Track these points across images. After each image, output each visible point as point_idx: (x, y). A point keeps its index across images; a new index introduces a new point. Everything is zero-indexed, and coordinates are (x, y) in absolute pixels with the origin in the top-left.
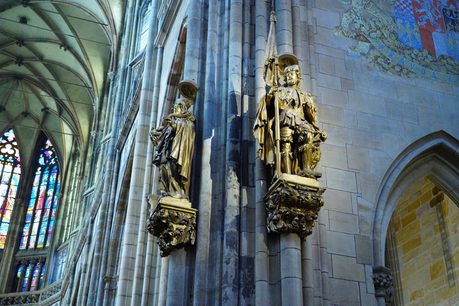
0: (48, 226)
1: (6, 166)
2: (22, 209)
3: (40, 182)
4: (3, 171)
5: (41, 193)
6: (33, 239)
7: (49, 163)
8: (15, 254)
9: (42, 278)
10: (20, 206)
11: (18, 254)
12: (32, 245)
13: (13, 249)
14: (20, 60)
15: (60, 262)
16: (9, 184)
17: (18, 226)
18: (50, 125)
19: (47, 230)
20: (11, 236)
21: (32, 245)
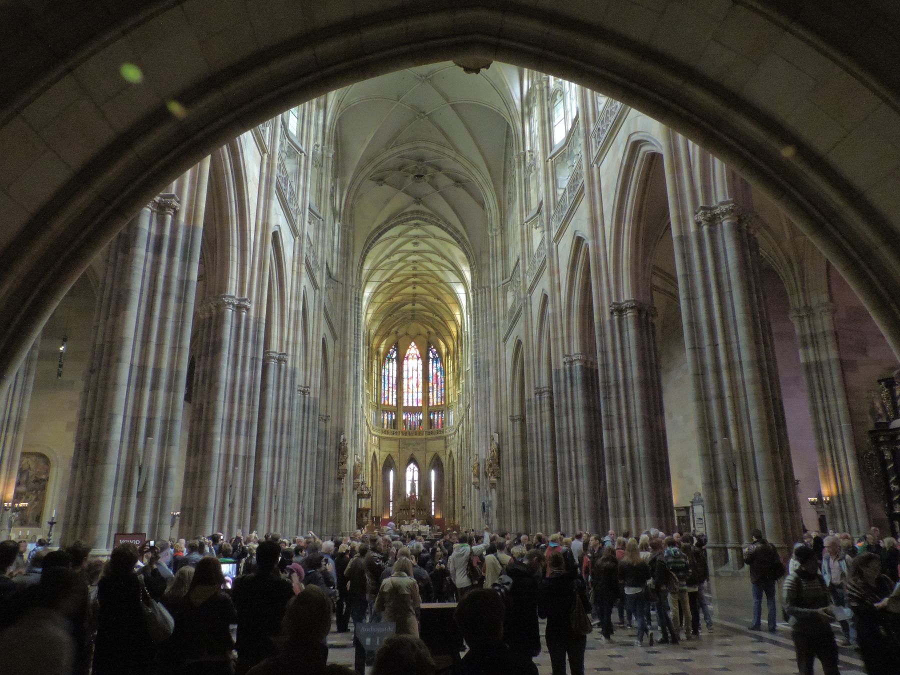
6: (435, 400)
18: (433, 338)
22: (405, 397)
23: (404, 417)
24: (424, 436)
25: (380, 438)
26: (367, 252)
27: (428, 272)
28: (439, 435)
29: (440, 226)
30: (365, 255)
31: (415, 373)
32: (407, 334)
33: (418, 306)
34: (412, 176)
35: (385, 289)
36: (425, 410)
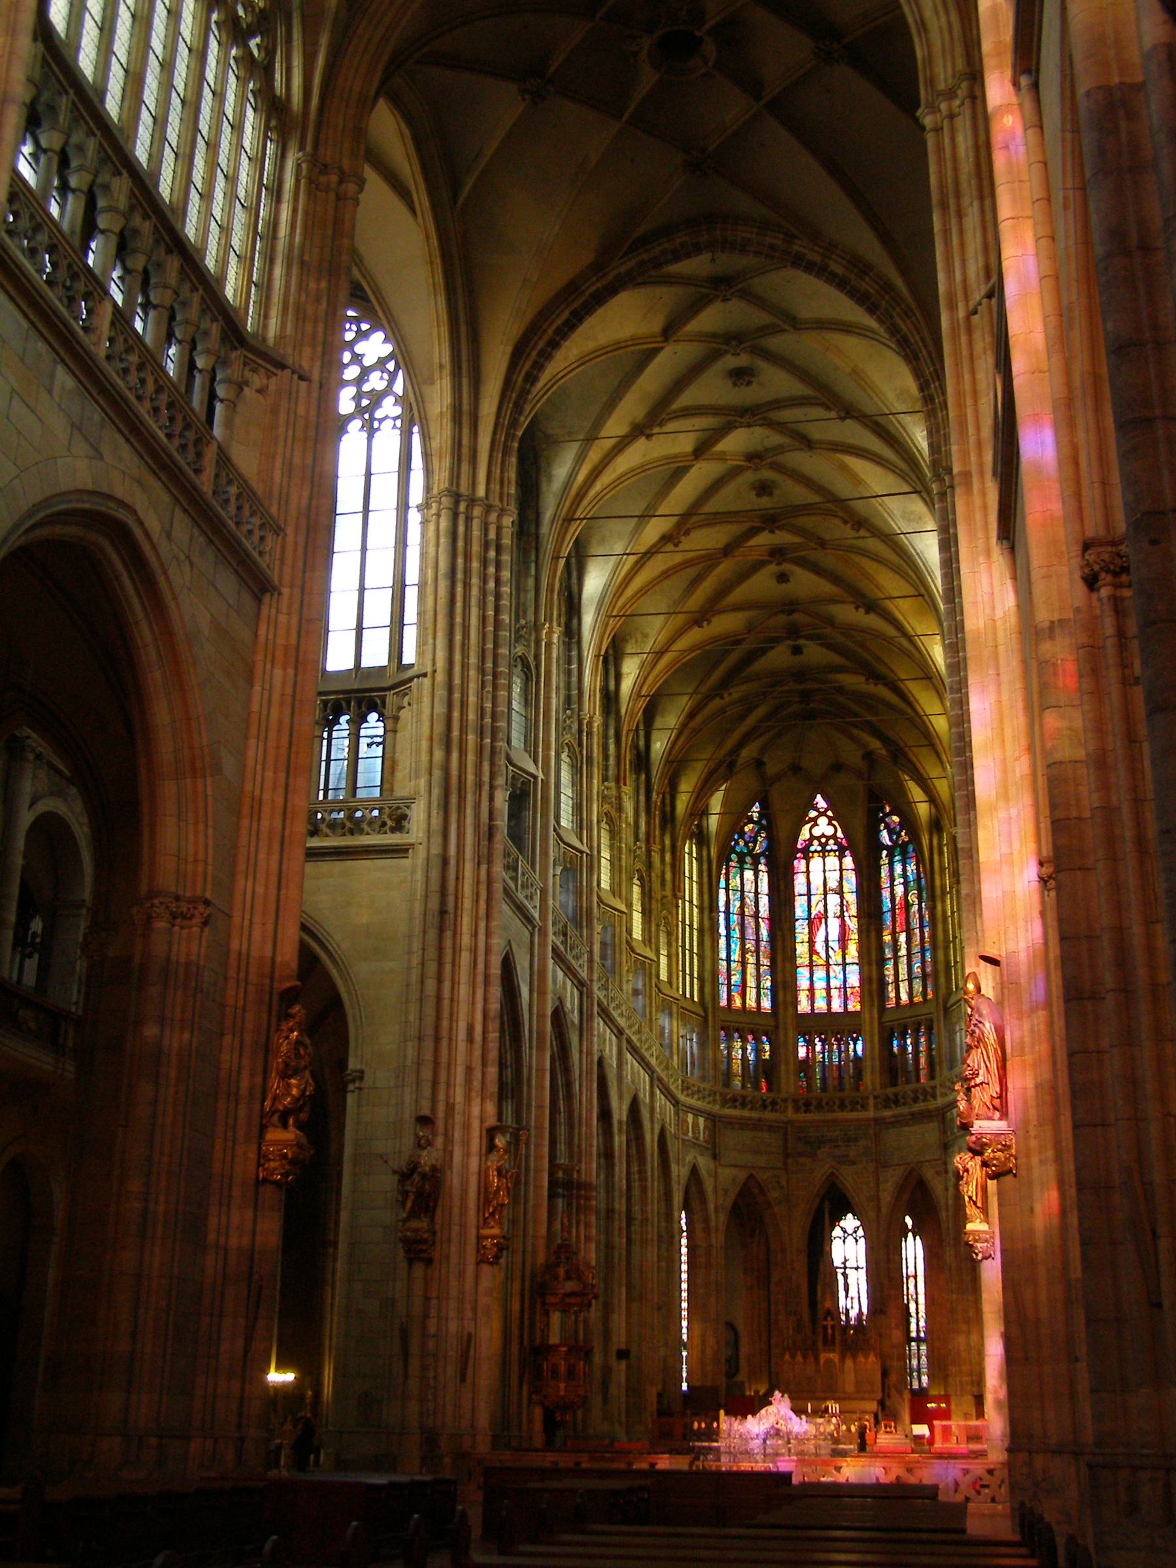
0: (923, 961)
1: (827, 859)
2: (873, 935)
3: (892, 878)
4: (824, 871)
5: (898, 899)
6: (904, 988)
7: (897, 838)
8: (880, 1018)
9: (934, 1053)
10: (868, 931)
11: (886, 1019)
12: (904, 997)
13: (875, 1011)
14: (806, 696)
15: (958, 1028)
16: (840, 892)
17: (874, 967)
19: (923, 967)
20: (866, 987)
21: (904, 997)
22: (803, 983)
23: (802, 1052)
24: (871, 1113)
25: (712, 1118)
26: (531, 379)
27: (813, 498)
28: (918, 1107)
29: (798, 262)
30: (524, 393)
31: (833, 900)
32: (796, 769)
33: (814, 654)
34: (646, 43)
35: (666, 575)
36: (870, 1023)
